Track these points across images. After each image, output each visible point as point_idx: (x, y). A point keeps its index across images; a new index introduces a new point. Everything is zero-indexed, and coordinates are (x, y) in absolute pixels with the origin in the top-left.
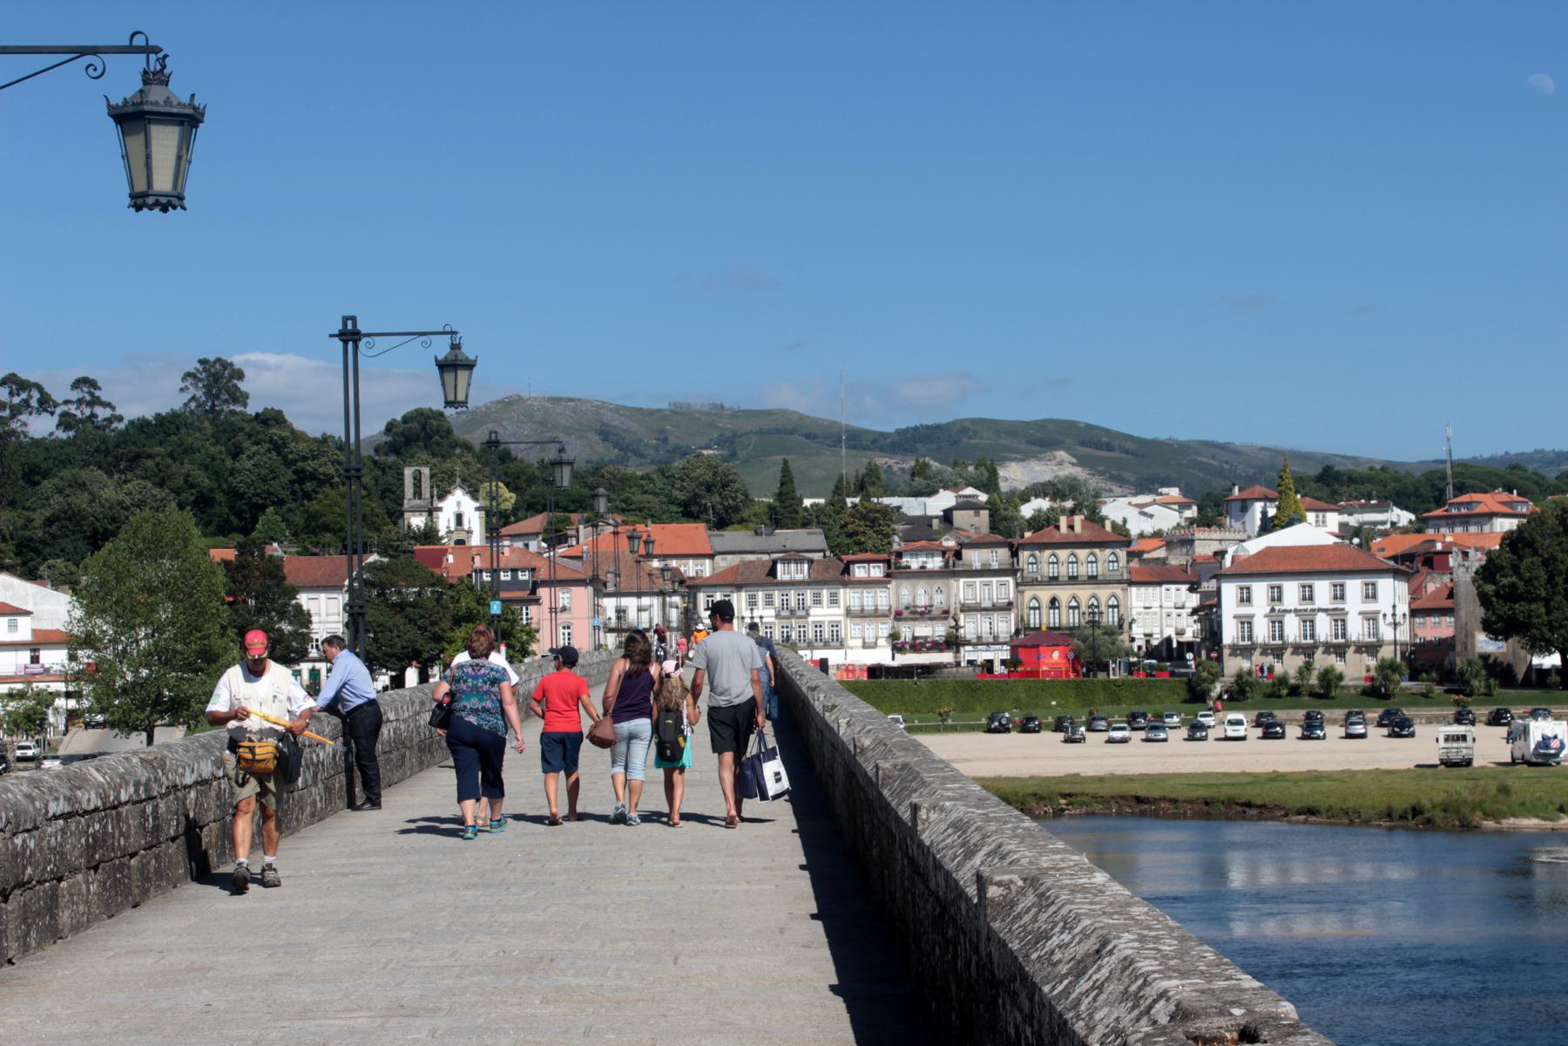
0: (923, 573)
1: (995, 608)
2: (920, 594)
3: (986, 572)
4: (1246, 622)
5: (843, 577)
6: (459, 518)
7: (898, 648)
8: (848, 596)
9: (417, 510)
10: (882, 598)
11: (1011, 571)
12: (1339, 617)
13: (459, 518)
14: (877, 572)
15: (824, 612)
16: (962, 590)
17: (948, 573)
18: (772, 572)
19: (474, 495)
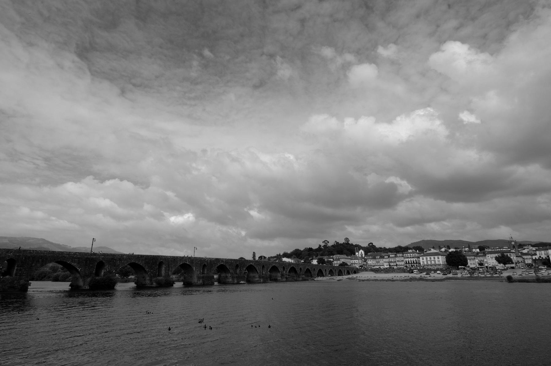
4: (423, 262)
8: (385, 260)
9: (357, 252)
12: (435, 261)
14: (387, 257)
16: (397, 259)
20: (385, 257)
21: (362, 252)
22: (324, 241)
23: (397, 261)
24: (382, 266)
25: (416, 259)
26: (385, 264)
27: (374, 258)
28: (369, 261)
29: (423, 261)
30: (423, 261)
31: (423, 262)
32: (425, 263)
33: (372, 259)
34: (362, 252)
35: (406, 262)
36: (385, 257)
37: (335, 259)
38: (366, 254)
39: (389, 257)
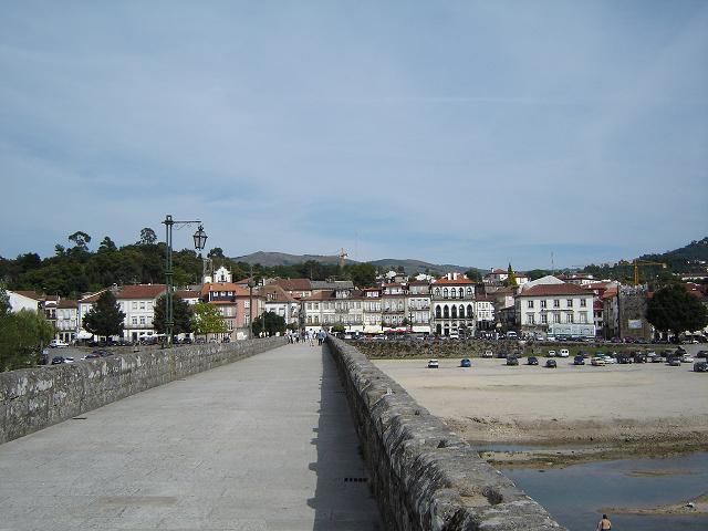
0: (391, 296)
1: (423, 309)
2: (394, 305)
3: (419, 295)
4: (531, 315)
5: (362, 297)
6: (223, 277)
7: (383, 325)
8: (366, 305)
9: (207, 274)
10: (378, 305)
11: (429, 295)
12: (570, 313)
13: (223, 277)
14: (376, 294)
15: (356, 309)
17: (405, 296)
18: (334, 295)
19: (228, 269)
20: (369, 295)
21: (223, 273)
22: (76, 234)
23: (407, 309)
24: (355, 324)
25: (472, 304)
26: (367, 319)
27: (330, 297)
28: (310, 307)
29: (531, 310)
30: (531, 310)
31: (531, 315)
32: (538, 319)
33: (321, 301)
34: (223, 273)
35: (439, 314)
36: (369, 295)
37: (214, 299)
38: (235, 279)
39: (381, 296)
